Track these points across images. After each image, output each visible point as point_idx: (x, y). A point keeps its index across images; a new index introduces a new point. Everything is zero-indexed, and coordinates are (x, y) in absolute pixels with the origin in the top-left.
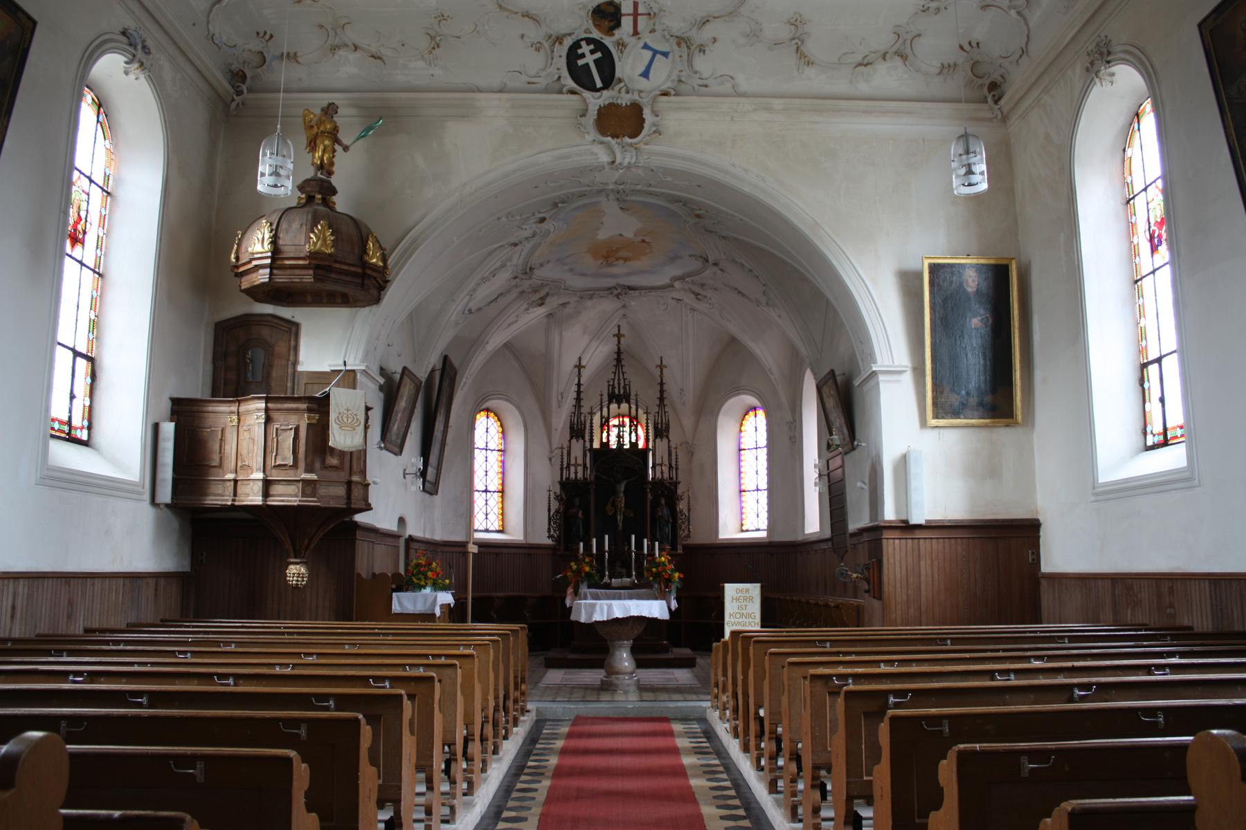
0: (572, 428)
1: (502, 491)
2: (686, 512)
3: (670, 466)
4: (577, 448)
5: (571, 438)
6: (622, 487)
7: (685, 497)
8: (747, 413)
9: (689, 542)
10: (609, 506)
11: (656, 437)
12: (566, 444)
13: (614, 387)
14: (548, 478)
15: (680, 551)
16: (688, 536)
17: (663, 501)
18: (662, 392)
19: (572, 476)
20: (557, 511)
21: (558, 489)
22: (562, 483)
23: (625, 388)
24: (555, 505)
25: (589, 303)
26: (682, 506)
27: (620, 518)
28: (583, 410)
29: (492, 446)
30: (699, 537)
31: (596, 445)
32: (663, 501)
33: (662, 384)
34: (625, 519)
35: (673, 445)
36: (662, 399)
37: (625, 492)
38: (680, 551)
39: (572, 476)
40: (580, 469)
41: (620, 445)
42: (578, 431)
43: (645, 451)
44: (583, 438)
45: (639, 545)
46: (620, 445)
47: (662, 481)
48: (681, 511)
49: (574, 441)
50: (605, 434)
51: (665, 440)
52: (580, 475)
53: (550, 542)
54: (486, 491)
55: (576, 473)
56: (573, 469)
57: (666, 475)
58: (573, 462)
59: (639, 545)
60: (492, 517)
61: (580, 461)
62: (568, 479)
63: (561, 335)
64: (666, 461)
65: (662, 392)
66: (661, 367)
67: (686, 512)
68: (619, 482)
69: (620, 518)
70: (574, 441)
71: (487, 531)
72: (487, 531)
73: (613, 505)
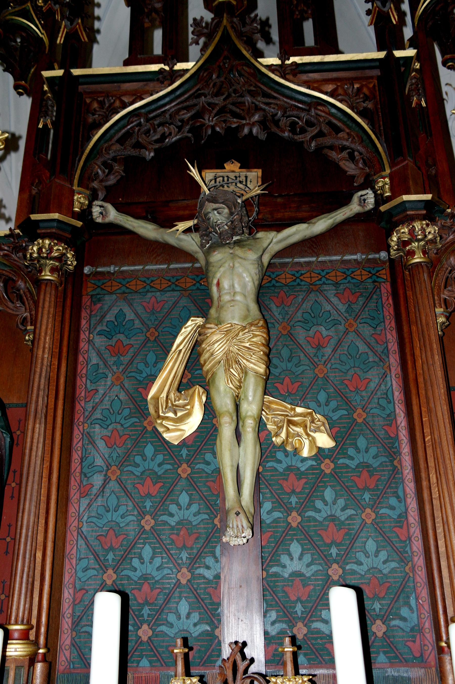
27: (238, 459)
69: (238, 459)
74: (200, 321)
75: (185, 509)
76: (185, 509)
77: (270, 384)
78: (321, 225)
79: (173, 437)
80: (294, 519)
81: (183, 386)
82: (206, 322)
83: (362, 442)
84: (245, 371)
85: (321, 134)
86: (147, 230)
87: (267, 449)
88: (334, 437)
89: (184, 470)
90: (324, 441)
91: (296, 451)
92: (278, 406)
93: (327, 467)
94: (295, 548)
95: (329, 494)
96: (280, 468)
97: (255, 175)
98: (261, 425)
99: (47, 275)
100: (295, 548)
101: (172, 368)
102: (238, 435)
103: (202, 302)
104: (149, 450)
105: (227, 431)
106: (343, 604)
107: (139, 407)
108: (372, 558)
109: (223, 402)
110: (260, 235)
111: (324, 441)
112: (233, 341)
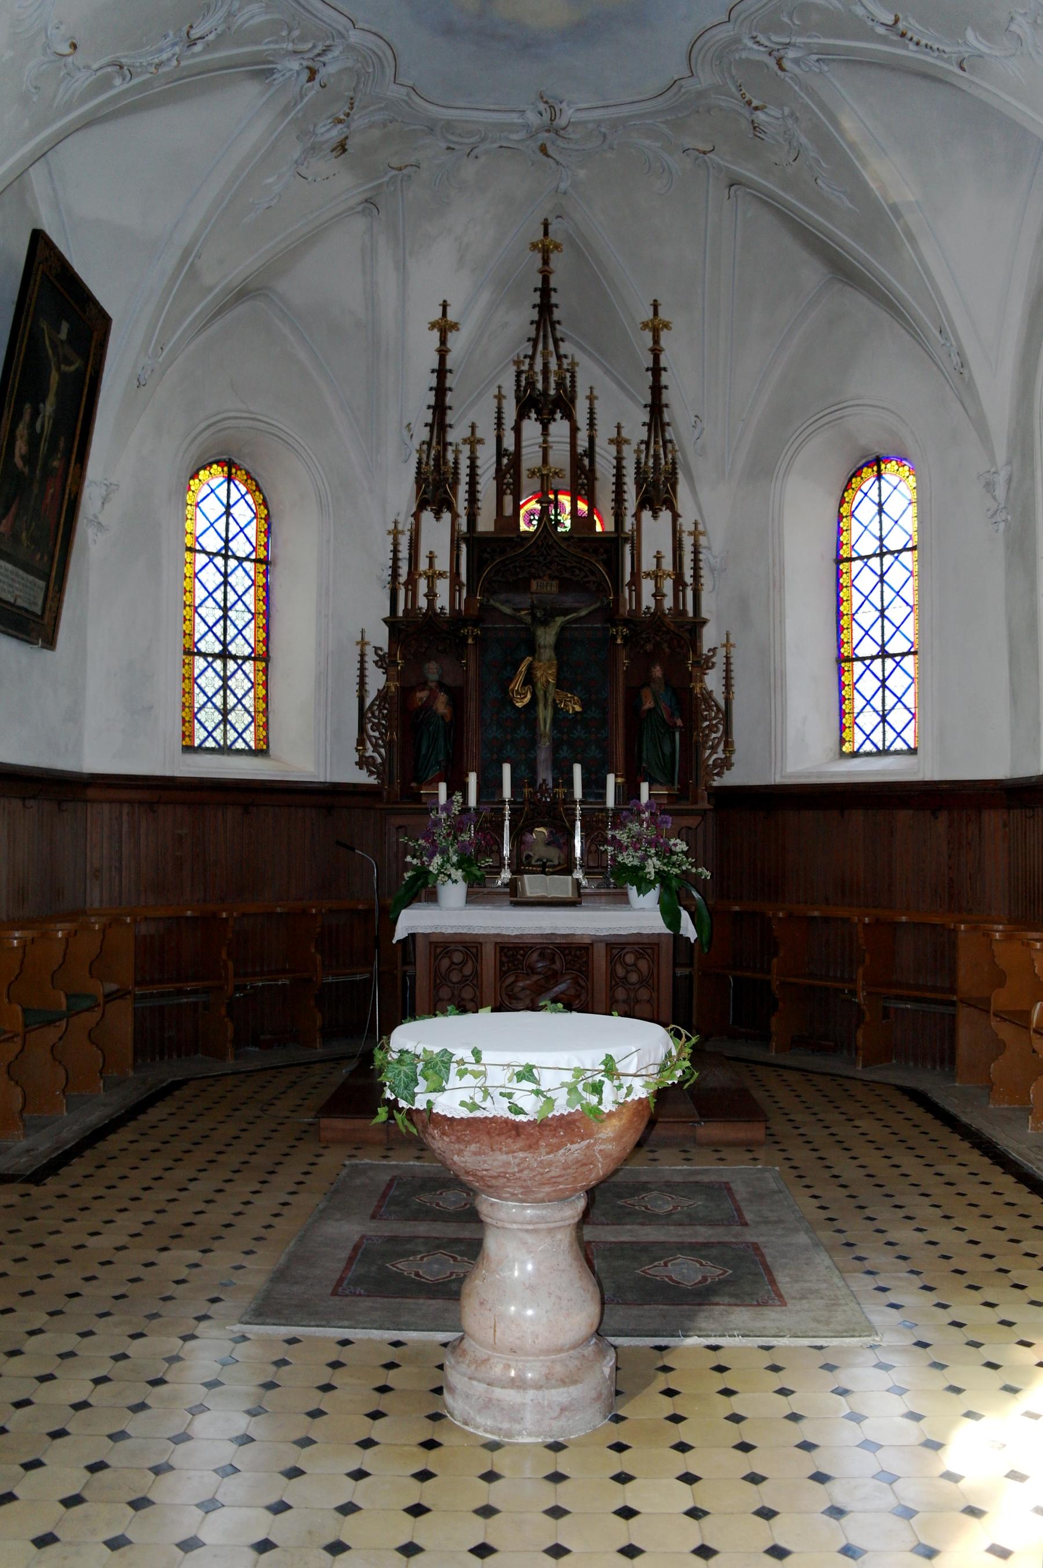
0: (420, 477)
1: (265, 658)
2: (719, 698)
3: (679, 582)
4: (437, 535)
5: (422, 506)
6: (547, 637)
7: (719, 659)
8: (858, 473)
9: (731, 779)
10: (517, 685)
11: (641, 507)
12: (406, 524)
13: (531, 384)
14: (370, 619)
15: (705, 805)
16: (726, 764)
17: (657, 672)
18: (657, 389)
19: (423, 603)
20: (383, 695)
21: (380, 637)
22: (392, 622)
23: (560, 385)
24: (377, 680)
25: (469, 171)
26: (713, 681)
28: (452, 436)
29: (240, 547)
30: (739, 775)
31: (486, 524)
32: (657, 672)
33: (656, 370)
34: (559, 718)
35: (686, 524)
36: (656, 407)
37: (559, 646)
38: (705, 805)
39: (423, 603)
40: (443, 587)
41: (547, 523)
42: (434, 490)
43: (612, 547)
44: (451, 508)
45: (594, 785)
46: (547, 523)
47: (657, 616)
48: (708, 696)
49: (427, 516)
50: (508, 499)
51: (666, 515)
52: (443, 601)
53: (364, 778)
54: (225, 655)
55: (431, 595)
56: (423, 585)
57: (668, 603)
58: (423, 565)
59: (594, 785)
60: (239, 718)
61: (443, 564)
62: (412, 609)
63: (402, 268)
64: (667, 565)
65: (657, 389)
66: (656, 328)
67: (719, 698)
68: (545, 623)
69: (545, 715)
70: (427, 516)
71: (225, 750)
72: (225, 750)
73: (529, 680)
74: (529, 659)
75: (522, 732)
76: (522, 732)
77: (559, 685)
78: (583, 613)
79: (519, 705)
80: (565, 737)
81: (524, 684)
82: (534, 659)
83: (593, 709)
84: (548, 682)
85: (586, 576)
86: (507, 610)
87: (556, 710)
88: (582, 706)
89: (523, 717)
90: (578, 709)
91: (568, 711)
92: (562, 694)
93: (579, 717)
94: (565, 748)
95: (579, 728)
96: (561, 717)
97: (554, 583)
98: (554, 700)
99: (470, 641)
100: (565, 748)
101: (520, 679)
102: (545, 706)
103: (532, 647)
104: (509, 708)
105: (541, 706)
106: (577, 769)
107: (504, 688)
108: (594, 752)
109: (540, 694)
110: (557, 619)
111: (578, 709)
112: (546, 674)
